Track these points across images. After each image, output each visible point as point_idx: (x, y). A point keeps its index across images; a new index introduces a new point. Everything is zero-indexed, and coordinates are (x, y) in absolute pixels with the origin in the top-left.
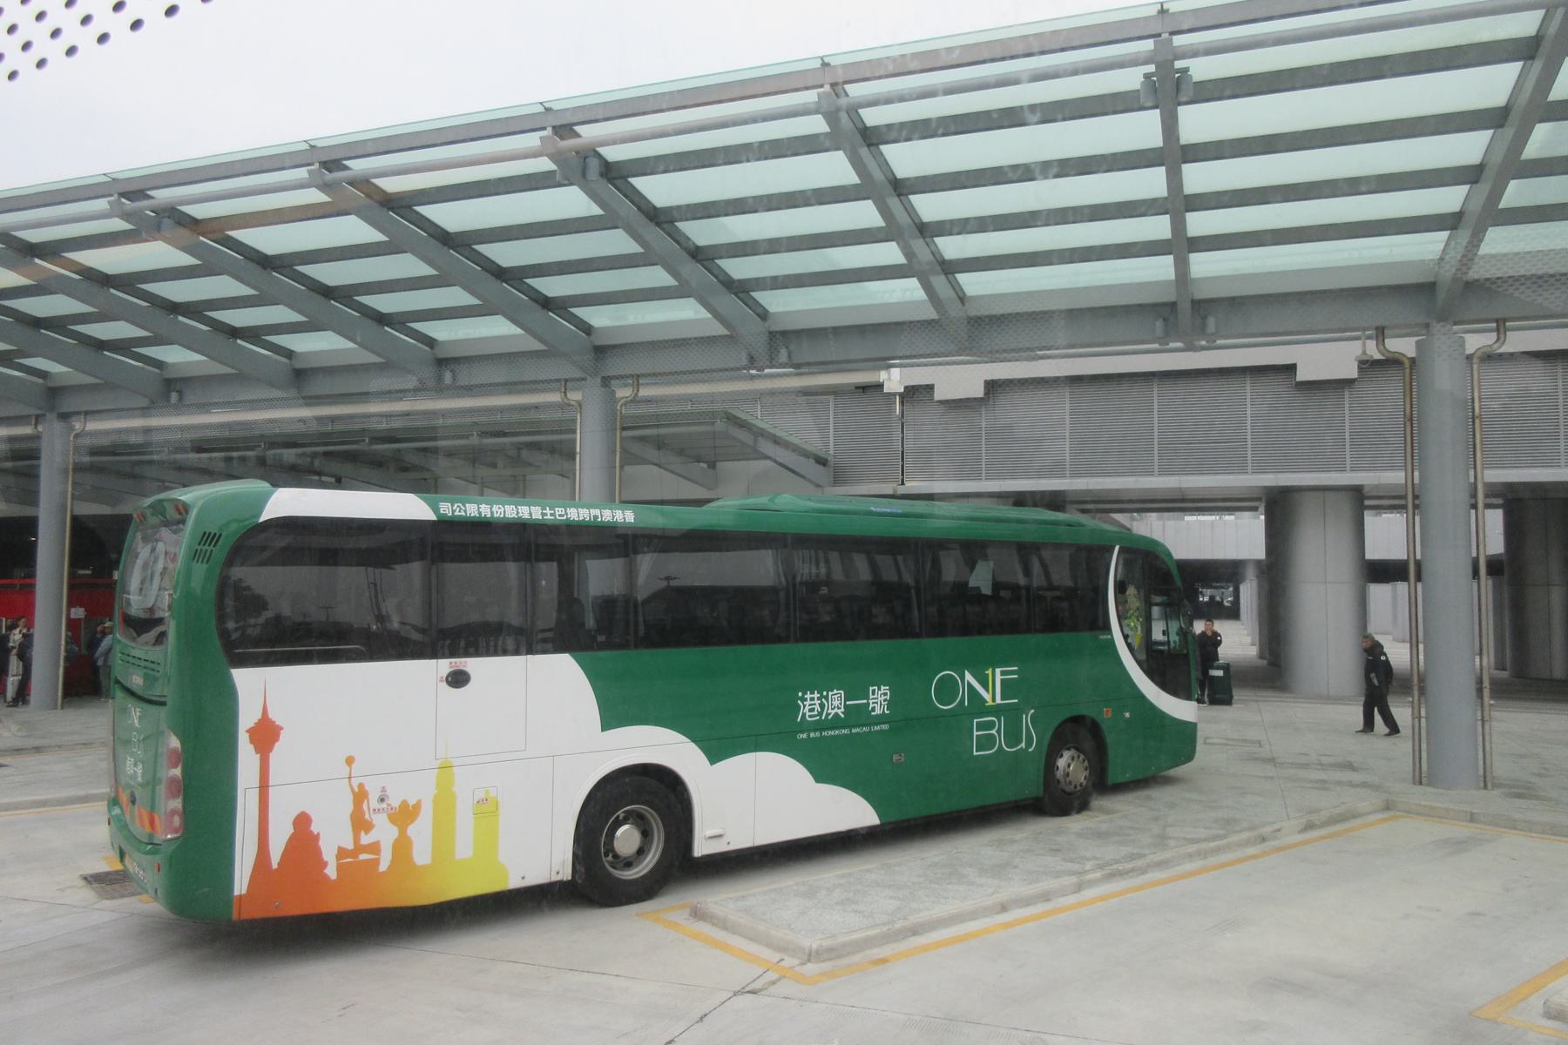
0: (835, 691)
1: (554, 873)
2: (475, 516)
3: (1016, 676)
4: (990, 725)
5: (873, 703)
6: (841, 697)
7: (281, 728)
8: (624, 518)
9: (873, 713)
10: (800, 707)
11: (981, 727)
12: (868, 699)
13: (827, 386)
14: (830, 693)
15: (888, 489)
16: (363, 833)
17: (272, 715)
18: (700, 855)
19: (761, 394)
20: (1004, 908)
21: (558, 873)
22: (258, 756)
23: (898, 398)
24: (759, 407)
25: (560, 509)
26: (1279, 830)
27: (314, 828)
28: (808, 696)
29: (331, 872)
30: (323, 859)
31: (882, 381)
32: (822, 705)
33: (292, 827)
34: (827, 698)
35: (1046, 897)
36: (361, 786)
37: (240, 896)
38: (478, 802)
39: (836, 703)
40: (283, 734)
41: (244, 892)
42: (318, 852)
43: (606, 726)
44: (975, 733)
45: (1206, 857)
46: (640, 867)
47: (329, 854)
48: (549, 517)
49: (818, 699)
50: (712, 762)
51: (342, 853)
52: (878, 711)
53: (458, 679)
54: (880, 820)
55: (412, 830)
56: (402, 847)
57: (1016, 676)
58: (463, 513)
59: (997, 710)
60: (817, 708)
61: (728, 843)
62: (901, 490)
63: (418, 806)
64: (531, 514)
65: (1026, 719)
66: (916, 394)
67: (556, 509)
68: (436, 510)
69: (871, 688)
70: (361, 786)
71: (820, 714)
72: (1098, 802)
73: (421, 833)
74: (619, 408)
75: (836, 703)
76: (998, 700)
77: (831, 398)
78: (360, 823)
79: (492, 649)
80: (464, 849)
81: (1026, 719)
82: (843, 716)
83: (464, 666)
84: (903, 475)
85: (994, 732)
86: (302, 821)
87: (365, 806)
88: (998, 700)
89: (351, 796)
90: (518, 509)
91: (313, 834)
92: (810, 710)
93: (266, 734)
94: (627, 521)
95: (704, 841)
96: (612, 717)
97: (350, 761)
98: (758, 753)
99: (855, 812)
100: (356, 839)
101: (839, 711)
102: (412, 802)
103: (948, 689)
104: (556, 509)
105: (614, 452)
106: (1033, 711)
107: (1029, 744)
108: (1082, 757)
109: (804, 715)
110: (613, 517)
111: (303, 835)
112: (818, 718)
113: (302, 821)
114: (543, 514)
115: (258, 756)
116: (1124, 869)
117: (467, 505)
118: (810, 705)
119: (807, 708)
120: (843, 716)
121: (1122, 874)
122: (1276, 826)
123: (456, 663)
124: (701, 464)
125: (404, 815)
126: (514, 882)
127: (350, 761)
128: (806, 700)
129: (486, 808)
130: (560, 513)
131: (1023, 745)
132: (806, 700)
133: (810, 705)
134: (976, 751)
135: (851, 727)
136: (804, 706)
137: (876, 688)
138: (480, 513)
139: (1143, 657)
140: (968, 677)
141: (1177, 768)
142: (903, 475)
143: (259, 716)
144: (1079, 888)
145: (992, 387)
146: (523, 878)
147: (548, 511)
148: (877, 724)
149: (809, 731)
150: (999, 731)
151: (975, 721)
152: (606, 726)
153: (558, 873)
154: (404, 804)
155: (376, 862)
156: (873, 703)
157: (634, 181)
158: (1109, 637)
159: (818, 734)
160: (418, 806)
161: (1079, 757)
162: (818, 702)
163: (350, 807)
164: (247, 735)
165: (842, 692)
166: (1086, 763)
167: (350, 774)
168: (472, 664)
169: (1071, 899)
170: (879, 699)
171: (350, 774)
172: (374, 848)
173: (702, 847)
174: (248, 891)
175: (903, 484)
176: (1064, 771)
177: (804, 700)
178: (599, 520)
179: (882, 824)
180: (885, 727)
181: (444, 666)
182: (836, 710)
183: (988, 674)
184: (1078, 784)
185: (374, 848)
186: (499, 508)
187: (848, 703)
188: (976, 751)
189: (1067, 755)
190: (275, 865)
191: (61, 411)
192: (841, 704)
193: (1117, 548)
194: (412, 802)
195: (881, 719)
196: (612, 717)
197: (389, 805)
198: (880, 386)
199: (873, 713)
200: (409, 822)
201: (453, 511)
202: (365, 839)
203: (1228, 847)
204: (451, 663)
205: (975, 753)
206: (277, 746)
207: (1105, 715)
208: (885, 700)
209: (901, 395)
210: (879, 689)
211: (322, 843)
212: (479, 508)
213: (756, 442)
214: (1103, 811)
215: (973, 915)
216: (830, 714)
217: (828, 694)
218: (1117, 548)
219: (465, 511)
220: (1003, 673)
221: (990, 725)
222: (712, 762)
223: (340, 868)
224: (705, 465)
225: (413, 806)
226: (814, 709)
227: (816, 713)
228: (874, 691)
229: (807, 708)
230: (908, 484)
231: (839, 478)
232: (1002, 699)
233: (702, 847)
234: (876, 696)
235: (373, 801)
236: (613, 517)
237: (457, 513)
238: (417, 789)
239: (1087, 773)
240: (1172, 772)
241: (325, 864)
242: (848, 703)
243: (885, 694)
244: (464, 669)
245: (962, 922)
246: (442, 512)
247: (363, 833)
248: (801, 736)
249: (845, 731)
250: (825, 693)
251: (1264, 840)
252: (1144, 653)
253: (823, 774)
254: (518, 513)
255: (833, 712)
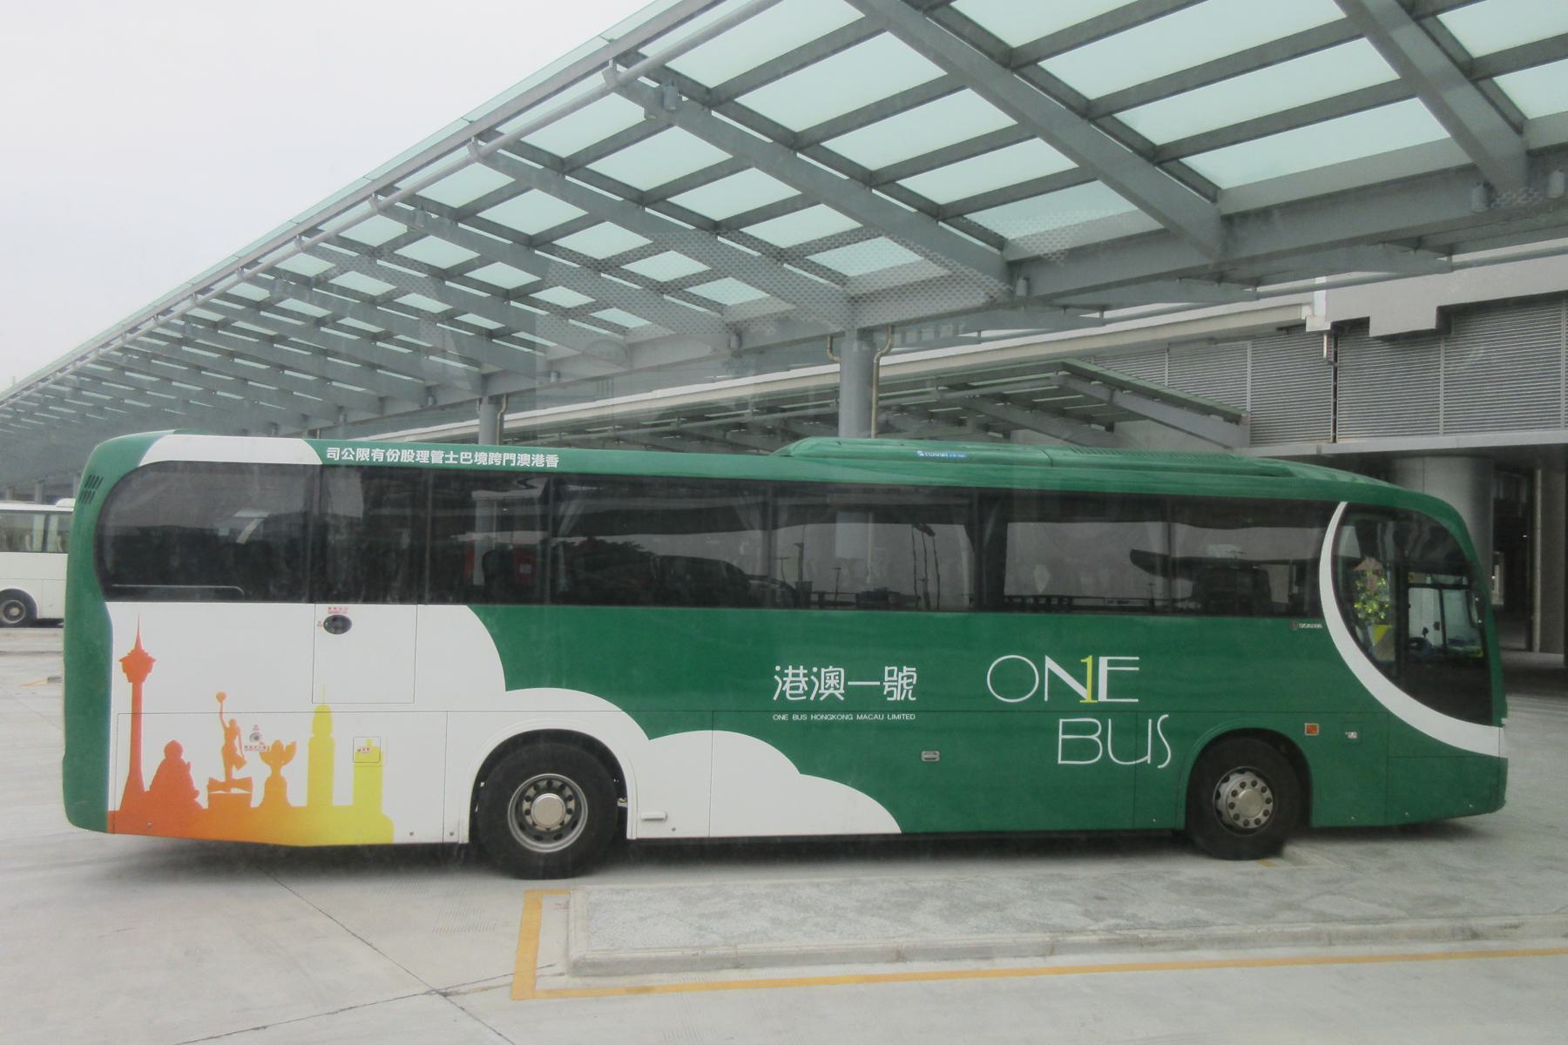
0: (831, 668)
1: (447, 834)
2: (365, 461)
3: (1137, 669)
4: (1091, 729)
5: (889, 687)
6: (839, 676)
7: (154, 660)
8: (545, 463)
9: (889, 699)
10: (778, 683)
11: (1069, 729)
12: (882, 680)
13: (1239, 330)
14: (823, 670)
15: (1310, 449)
16: (234, 769)
17: (145, 647)
18: (634, 838)
19: (1169, 344)
20: (900, 956)
21: (452, 834)
22: (131, 684)
23: (1325, 338)
24: (1167, 357)
25: (466, 453)
26: (1516, 927)
27: (185, 757)
28: (790, 671)
29: (203, 800)
30: (193, 788)
31: (1303, 318)
32: (810, 684)
33: (163, 753)
34: (818, 676)
35: (984, 953)
36: (232, 722)
37: (114, 813)
38: (359, 750)
39: (832, 682)
40: (155, 666)
41: (118, 808)
42: (188, 780)
43: (509, 687)
44: (1061, 737)
45: (1331, 944)
46: (567, 839)
47: (199, 782)
48: (451, 461)
49: (805, 675)
50: (650, 739)
51: (213, 785)
52: (897, 696)
53: (338, 625)
54: (901, 829)
55: (285, 771)
56: (275, 785)
57: (1137, 669)
58: (351, 458)
59: (1099, 710)
60: (803, 686)
61: (674, 829)
62: (1328, 449)
63: (292, 748)
64: (430, 458)
65: (1155, 726)
66: (1349, 331)
67: (462, 454)
68: (322, 455)
69: (887, 669)
70: (232, 722)
71: (808, 693)
72: (1298, 850)
73: (295, 775)
74: (875, 362)
75: (832, 682)
76: (1103, 696)
77: (1249, 343)
78: (231, 758)
79: (427, 596)
80: (343, 792)
81: (1155, 726)
82: (842, 698)
83: (345, 612)
84: (1335, 430)
85: (1094, 737)
86: (173, 750)
87: (236, 742)
88: (1103, 696)
89: (222, 732)
90: (416, 453)
91: (184, 763)
92: (792, 688)
93: (138, 665)
94: (548, 466)
95: (640, 823)
96: (520, 674)
97: (221, 697)
98: (717, 733)
99: (875, 819)
100: (228, 773)
101: (837, 693)
102: (286, 743)
103: (1014, 679)
104: (462, 454)
105: (870, 408)
106: (1167, 716)
107: (1159, 754)
108: (1261, 784)
109: (783, 693)
110: (531, 461)
111: (174, 766)
112: (804, 698)
113: (173, 750)
114: (444, 459)
115: (131, 684)
116: (1145, 938)
117: (403, 451)
118: (791, 682)
119: (787, 686)
120: (842, 698)
121: (1141, 944)
122: (1514, 920)
123: (335, 608)
124: (1094, 426)
125: (278, 755)
126: (400, 836)
127: (221, 697)
128: (787, 675)
129: (368, 758)
130: (466, 457)
131: (1148, 758)
132: (787, 675)
133: (791, 682)
134: (1062, 759)
135: (855, 712)
136: (784, 683)
137: (896, 669)
138: (371, 458)
139: (1390, 657)
140: (1050, 664)
141: (1487, 815)
142: (1335, 430)
143: (132, 647)
144: (1052, 949)
145: (1454, 318)
146: (411, 834)
147: (452, 455)
148: (896, 712)
149: (791, 713)
150: (1103, 737)
151: (1061, 721)
152: (509, 687)
153: (452, 834)
154: (277, 745)
155: (248, 798)
156: (889, 687)
157: (741, 100)
158: (1319, 626)
159: (804, 717)
160: (292, 748)
161: (1254, 784)
162: (804, 680)
163: (222, 742)
164: (121, 664)
165: (842, 670)
166: (1268, 794)
167: (221, 709)
168: (351, 610)
169: (1039, 962)
170: (899, 682)
171: (221, 709)
172: (246, 783)
173: (636, 830)
174: (121, 807)
175: (1335, 441)
176: (1228, 797)
177: (782, 675)
178: (513, 465)
179: (903, 834)
180: (910, 717)
181: (323, 610)
182: (832, 691)
183: (1085, 664)
184: (1252, 821)
185: (246, 783)
186: (395, 452)
187: (849, 683)
188: (1062, 759)
189: (1235, 781)
190: (147, 788)
191: (491, 394)
192: (839, 684)
193: (1342, 506)
194: (286, 743)
195: (903, 706)
196: (520, 674)
197: (261, 743)
198: (1303, 325)
199: (889, 699)
200: (283, 762)
201: (341, 456)
202: (237, 774)
203: (1391, 936)
204: (330, 608)
205: (1060, 762)
206: (149, 677)
207: (1309, 732)
208: (908, 685)
209: (1329, 333)
210: (900, 670)
211: (193, 773)
212: (371, 452)
213: (1112, 396)
214: (1296, 861)
215: (844, 957)
216: (823, 694)
217: (819, 671)
218: (1342, 506)
219: (355, 456)
220: (1110, 663)
221: (1091, 729)
222: (650, 739)
223: (211, 798)
224: (1102, 428)
225: (288, 747)
226: (799, 687)
227: (801, 691)
228: (891, 674)
229: (787, 686)
230: (1340, 442)
231: (1256, 439)
232: (1110, 693)
233: (636, 830)
234: (895, 678)
235: (245, 738)
236: (531, 461)
237: (345, 458)
238: (296, 732)
239: (1270, 807)
240: (1464, 821)
241: (196, 794)
242: (849, 683)
243: (909, 677)
244: (345, 615)
245: (825, 963)
246: (328, 457)
247: (234, 769)
248: (779, 717)
249: (847, 717)
250: (815, 670)
251: (1475, 935)
252: (1392, 650)
253: (808, 763)
254: (415, 457)
255: (827, 693)
